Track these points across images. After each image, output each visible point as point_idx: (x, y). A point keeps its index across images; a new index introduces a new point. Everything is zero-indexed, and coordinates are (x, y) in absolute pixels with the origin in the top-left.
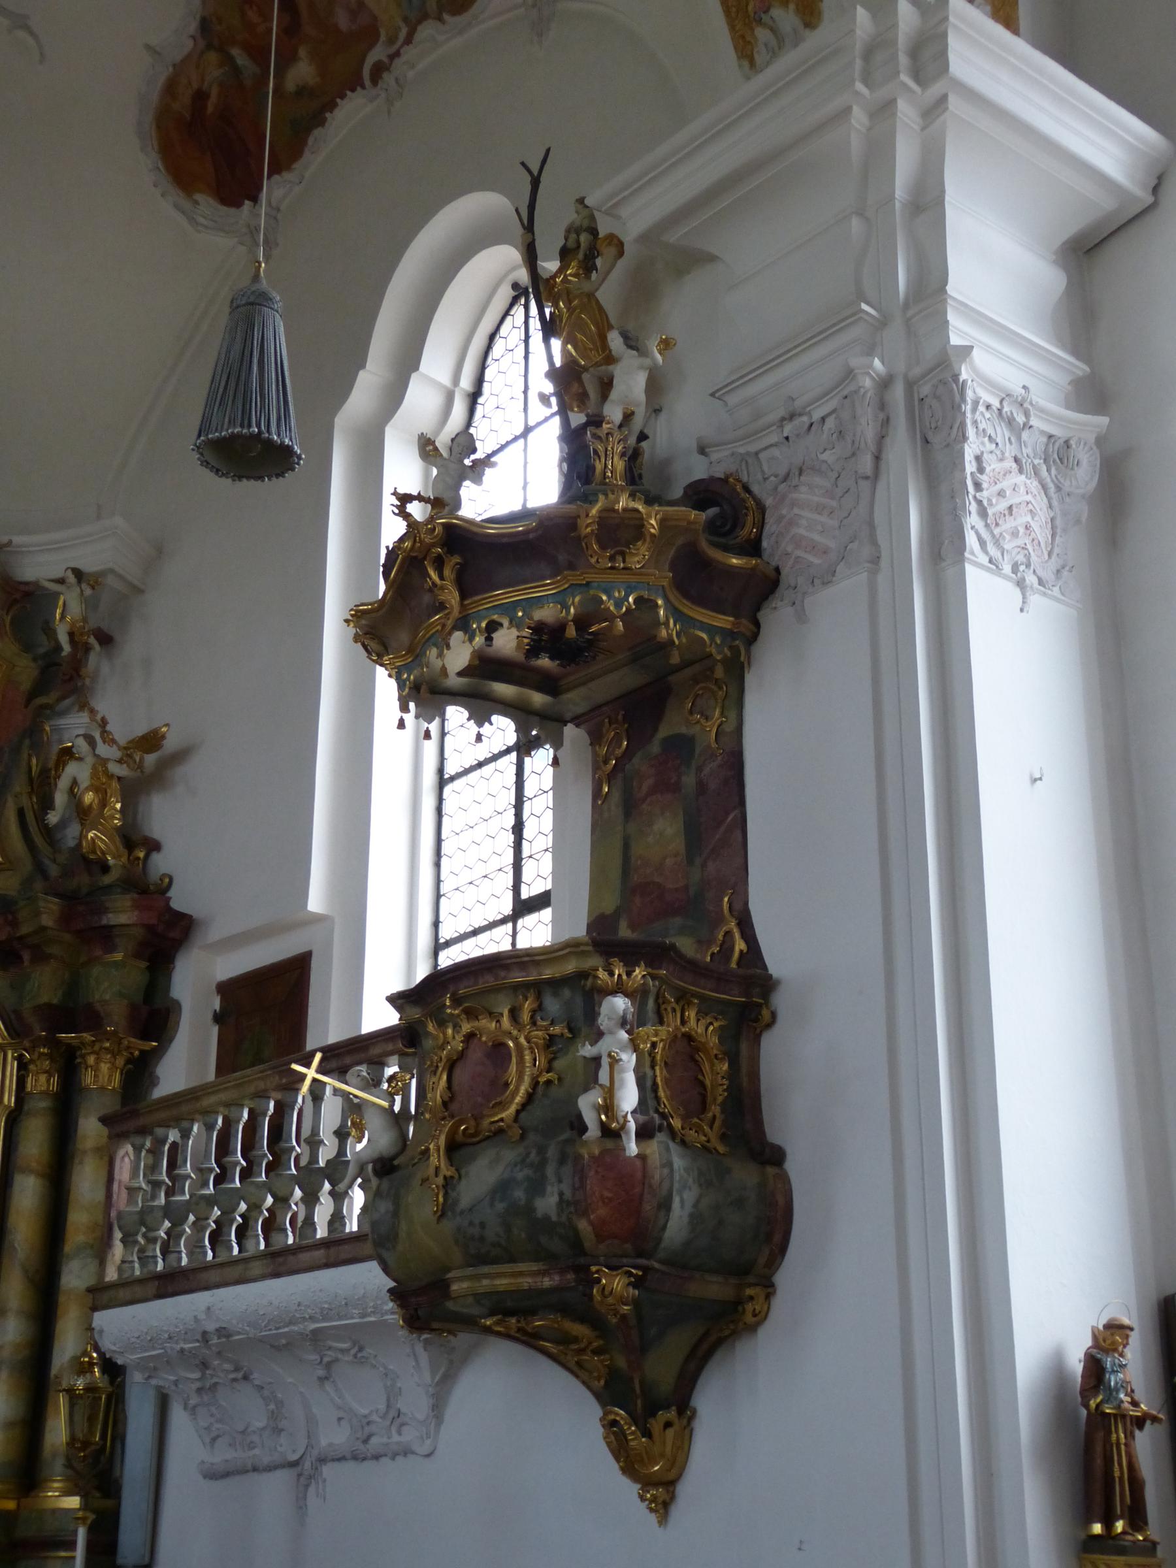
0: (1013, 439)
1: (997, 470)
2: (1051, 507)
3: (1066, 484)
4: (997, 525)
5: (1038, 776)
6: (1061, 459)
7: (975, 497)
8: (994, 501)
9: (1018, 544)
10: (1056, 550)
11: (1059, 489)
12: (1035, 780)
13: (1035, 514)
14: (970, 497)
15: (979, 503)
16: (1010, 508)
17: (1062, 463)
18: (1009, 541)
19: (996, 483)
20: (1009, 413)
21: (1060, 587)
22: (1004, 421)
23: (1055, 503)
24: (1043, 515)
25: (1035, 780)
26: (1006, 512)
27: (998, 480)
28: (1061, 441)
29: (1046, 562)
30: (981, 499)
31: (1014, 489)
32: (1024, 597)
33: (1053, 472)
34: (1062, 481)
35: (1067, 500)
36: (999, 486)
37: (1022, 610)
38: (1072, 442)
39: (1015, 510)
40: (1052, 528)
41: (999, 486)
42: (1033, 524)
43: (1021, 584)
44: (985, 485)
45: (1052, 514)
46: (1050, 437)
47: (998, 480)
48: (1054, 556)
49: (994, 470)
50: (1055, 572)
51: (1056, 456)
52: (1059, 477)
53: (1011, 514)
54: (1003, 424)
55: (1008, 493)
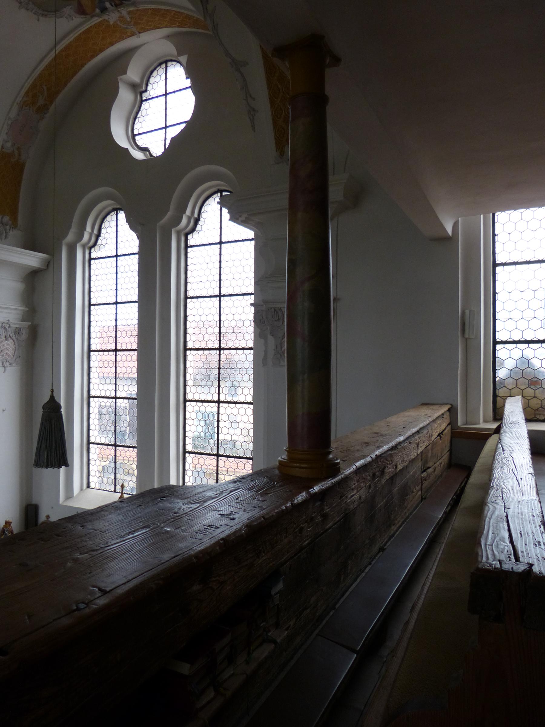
0: (5, 332)
2: (15, 345)
5: (4, 409)
6: (19, 333)
10: (15, 354)
11: (17, 339)
12: (4, 410)
22: (3, 328)
24: (13, 346)
25: (4, 410)
28: (19, 328)
33: (16, 336)
37: (4, 372)
38: (21, 329)
39: (3, 350)
42: (8, 353)
43: (4, 367)
45: (15, 346)
46: (16, 327)
48: (14, 357)
51: (17, 332)
53: (2, 352)
54: (3, 329)
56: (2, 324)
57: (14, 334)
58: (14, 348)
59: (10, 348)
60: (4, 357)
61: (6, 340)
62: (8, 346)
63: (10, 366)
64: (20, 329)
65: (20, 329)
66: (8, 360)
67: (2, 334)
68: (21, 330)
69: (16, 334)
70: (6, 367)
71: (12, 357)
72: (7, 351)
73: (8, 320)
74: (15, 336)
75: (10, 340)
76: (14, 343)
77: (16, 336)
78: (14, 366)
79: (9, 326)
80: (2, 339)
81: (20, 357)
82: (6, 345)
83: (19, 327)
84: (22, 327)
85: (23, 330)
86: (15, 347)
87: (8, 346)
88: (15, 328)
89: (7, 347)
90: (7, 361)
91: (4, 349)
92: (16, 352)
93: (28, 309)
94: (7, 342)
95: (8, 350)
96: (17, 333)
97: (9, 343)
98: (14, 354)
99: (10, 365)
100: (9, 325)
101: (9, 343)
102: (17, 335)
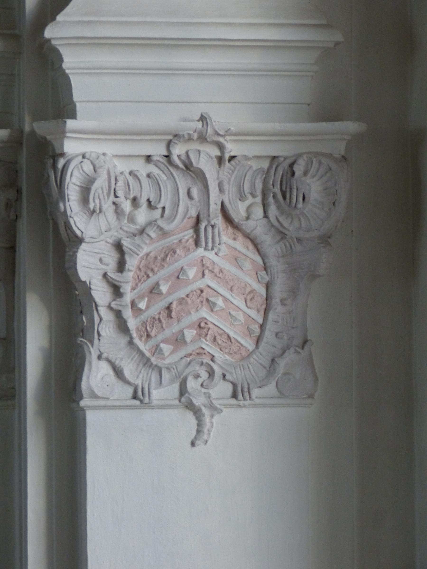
0: (195, 192)
1: (153, 254)
3: (291, 229)
4: (148, 336)
7: (110, 307)
8: (142, 305)
9: (189, 351)
10: (270, 328)
13: (214, 304)
14: (103, 311)
15: (118, 314)
16: (169, 308)
17: (284, 198)
18: (172, 353)
19: (148, 276)
20: (183, 157)
21: (277, 383)
22: (176, 167)
23: (273, 262)
26: (164, 314)
27: (152, 270)
29: (250, 355)
30: (120, 308)
31: (178, 277)
32: (200, 424)
33: (273, 211)
34: (286, 225)
35: (298, 248)
36: (153, 279)
37: (193, 444)
38: (299, 169)
40: (267, 299)
41: (153, 279)
44: (126, 288)
45: (267, 278)
46: (274, 158)
47: (152, 270)
48: (263, 345)
49: (147, 255)
50: (267, 366)
51: (277, 190)
52: (281, 219)
53: (170, 316)
55: (164, 288)
56: (169, 144)
57: (259, 199)
58: (263, 291)
59: (227, 295)
60: (190, 349)
61: (197, 243)
62: (208, 280)
63: (234, 401)
64: (291, 165)
65: (291, 165)
66: (216, 368)
67: (176, 205)
68: (293, 174)
69: (271, 199)
70: (205, 410)
71: (249, 345)
72: (205, 313)
73: (203, 118)
74: (266, 216)
75: (224, 238)
76: (259, 260)
77: (273, 211)
78: (265, 406)
79: (217, 153)
80: (173, 239)
81: (305, 342)
82: (192, 273)
83: (285, 158)
84: (300, 155)
85: (306, 173)
86: (268, 286)
87: (208, 280)
88: (265, 165)
89: (200, 284)
90: (211, 374)
91: (181, 301)
92: (271, 316)
93: (339, 37)
94: (201, 251)
95: (212, 306)
96: (274, 196)
97: (215, 259)
98: (262, 327)
99: (234, 396)
100: (221, 147)
101: (215, 259)
102: (279, 207)
